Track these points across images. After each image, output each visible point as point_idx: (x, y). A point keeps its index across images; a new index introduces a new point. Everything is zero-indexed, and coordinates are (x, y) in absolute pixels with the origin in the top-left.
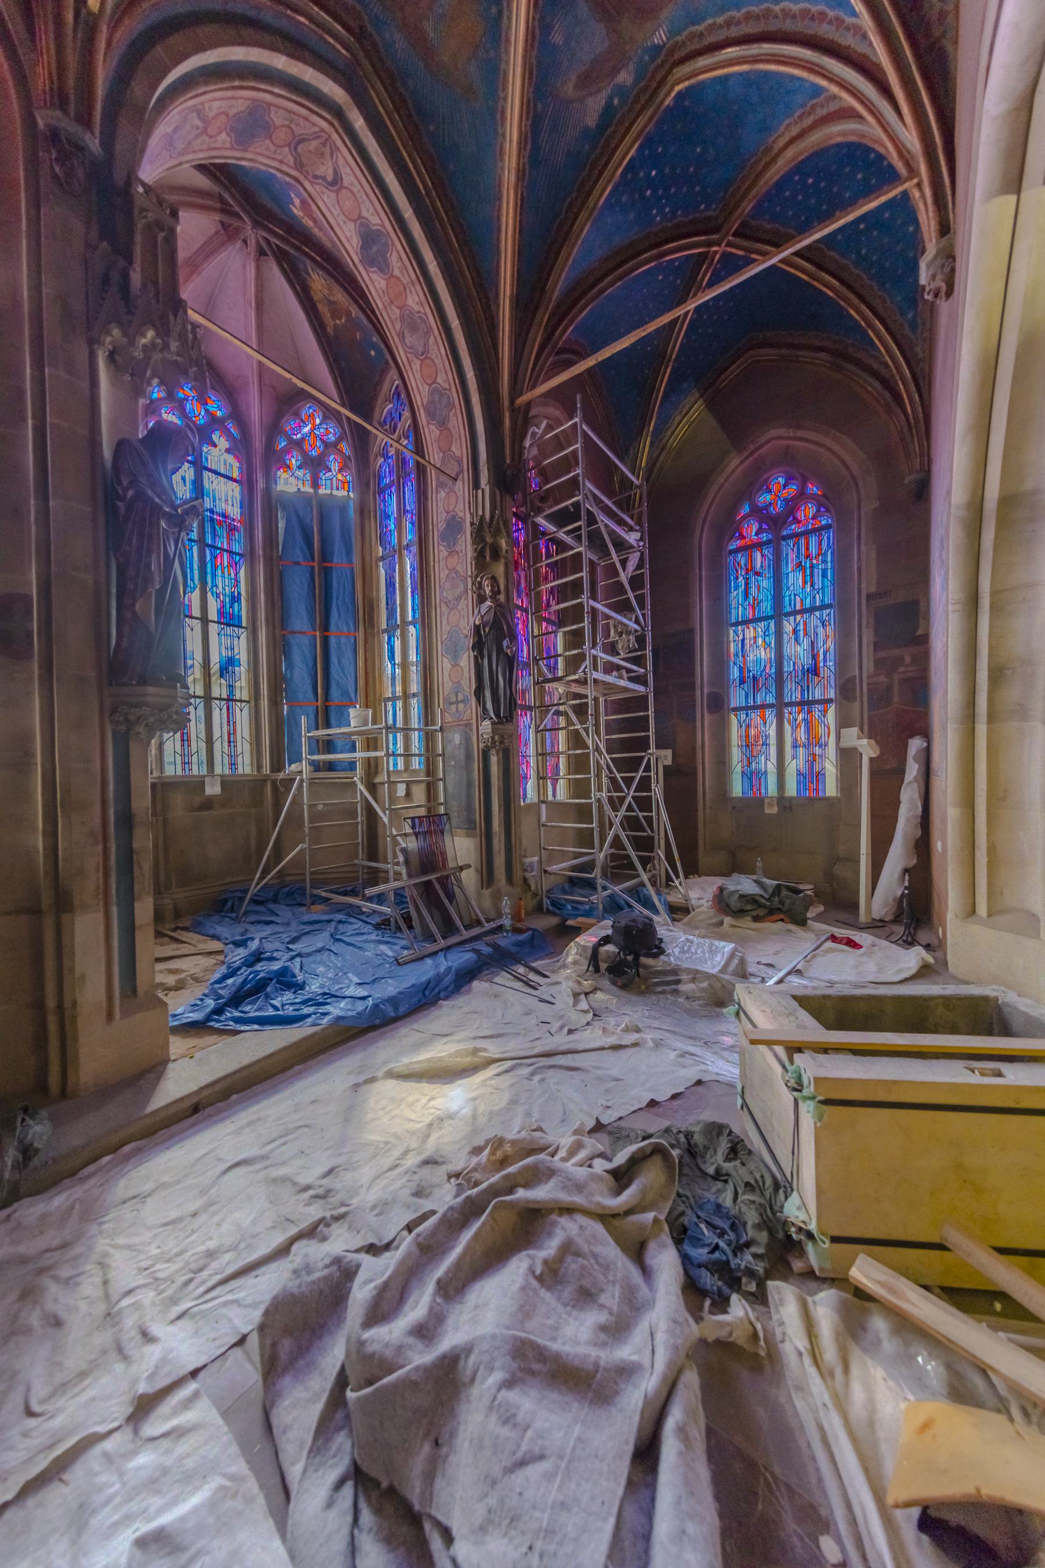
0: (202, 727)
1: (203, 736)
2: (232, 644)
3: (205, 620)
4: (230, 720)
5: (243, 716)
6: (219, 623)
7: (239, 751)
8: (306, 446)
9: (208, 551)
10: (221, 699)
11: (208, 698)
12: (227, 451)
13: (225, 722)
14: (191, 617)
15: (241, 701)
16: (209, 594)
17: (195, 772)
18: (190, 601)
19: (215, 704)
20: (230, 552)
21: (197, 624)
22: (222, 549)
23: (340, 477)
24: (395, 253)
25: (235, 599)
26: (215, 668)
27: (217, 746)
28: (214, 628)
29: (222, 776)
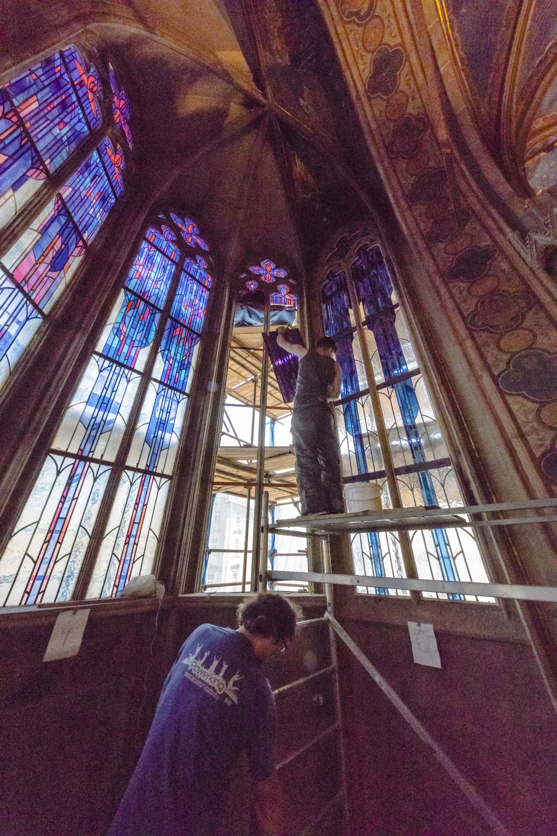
0: (94, 509)
1: (90, 525)
2: (170, 407)
3: (146, 376)
4: (140, 504)
5: (159, 496)
6: (160, 382)
7: (139, 553)
8: (263, 278)
9: (169, 321)
10: (136, 470)
11: (118, 467)
12: (205, 270)
13: (132, 504)
14: (132, 369)
15: (162, 475)
16: (159, 356)
17: (49, 598)
18: (137, 353)
19: (126, 477)
20: (189, 329)
21: (136, 380)
22: (183, 325)
23: (287, 297)
24: (407, 69)
25: (184, 366)
26: (142, 429)
27: (107, 543)
28: (153, 388)
29: (97, 606)
